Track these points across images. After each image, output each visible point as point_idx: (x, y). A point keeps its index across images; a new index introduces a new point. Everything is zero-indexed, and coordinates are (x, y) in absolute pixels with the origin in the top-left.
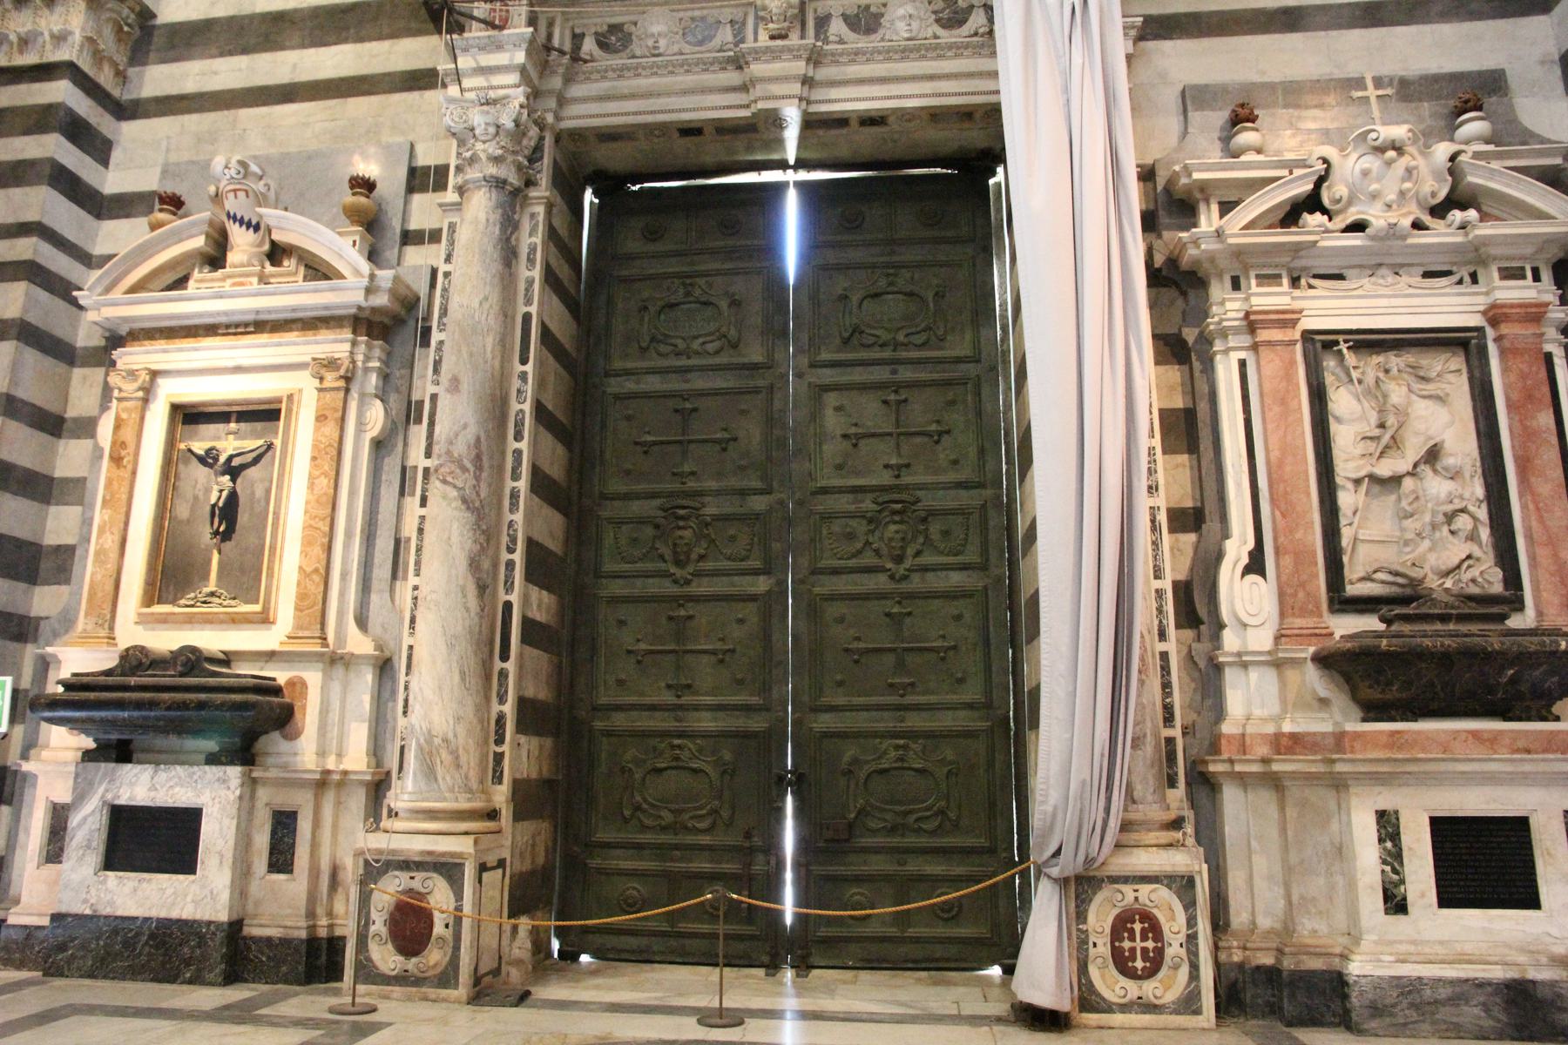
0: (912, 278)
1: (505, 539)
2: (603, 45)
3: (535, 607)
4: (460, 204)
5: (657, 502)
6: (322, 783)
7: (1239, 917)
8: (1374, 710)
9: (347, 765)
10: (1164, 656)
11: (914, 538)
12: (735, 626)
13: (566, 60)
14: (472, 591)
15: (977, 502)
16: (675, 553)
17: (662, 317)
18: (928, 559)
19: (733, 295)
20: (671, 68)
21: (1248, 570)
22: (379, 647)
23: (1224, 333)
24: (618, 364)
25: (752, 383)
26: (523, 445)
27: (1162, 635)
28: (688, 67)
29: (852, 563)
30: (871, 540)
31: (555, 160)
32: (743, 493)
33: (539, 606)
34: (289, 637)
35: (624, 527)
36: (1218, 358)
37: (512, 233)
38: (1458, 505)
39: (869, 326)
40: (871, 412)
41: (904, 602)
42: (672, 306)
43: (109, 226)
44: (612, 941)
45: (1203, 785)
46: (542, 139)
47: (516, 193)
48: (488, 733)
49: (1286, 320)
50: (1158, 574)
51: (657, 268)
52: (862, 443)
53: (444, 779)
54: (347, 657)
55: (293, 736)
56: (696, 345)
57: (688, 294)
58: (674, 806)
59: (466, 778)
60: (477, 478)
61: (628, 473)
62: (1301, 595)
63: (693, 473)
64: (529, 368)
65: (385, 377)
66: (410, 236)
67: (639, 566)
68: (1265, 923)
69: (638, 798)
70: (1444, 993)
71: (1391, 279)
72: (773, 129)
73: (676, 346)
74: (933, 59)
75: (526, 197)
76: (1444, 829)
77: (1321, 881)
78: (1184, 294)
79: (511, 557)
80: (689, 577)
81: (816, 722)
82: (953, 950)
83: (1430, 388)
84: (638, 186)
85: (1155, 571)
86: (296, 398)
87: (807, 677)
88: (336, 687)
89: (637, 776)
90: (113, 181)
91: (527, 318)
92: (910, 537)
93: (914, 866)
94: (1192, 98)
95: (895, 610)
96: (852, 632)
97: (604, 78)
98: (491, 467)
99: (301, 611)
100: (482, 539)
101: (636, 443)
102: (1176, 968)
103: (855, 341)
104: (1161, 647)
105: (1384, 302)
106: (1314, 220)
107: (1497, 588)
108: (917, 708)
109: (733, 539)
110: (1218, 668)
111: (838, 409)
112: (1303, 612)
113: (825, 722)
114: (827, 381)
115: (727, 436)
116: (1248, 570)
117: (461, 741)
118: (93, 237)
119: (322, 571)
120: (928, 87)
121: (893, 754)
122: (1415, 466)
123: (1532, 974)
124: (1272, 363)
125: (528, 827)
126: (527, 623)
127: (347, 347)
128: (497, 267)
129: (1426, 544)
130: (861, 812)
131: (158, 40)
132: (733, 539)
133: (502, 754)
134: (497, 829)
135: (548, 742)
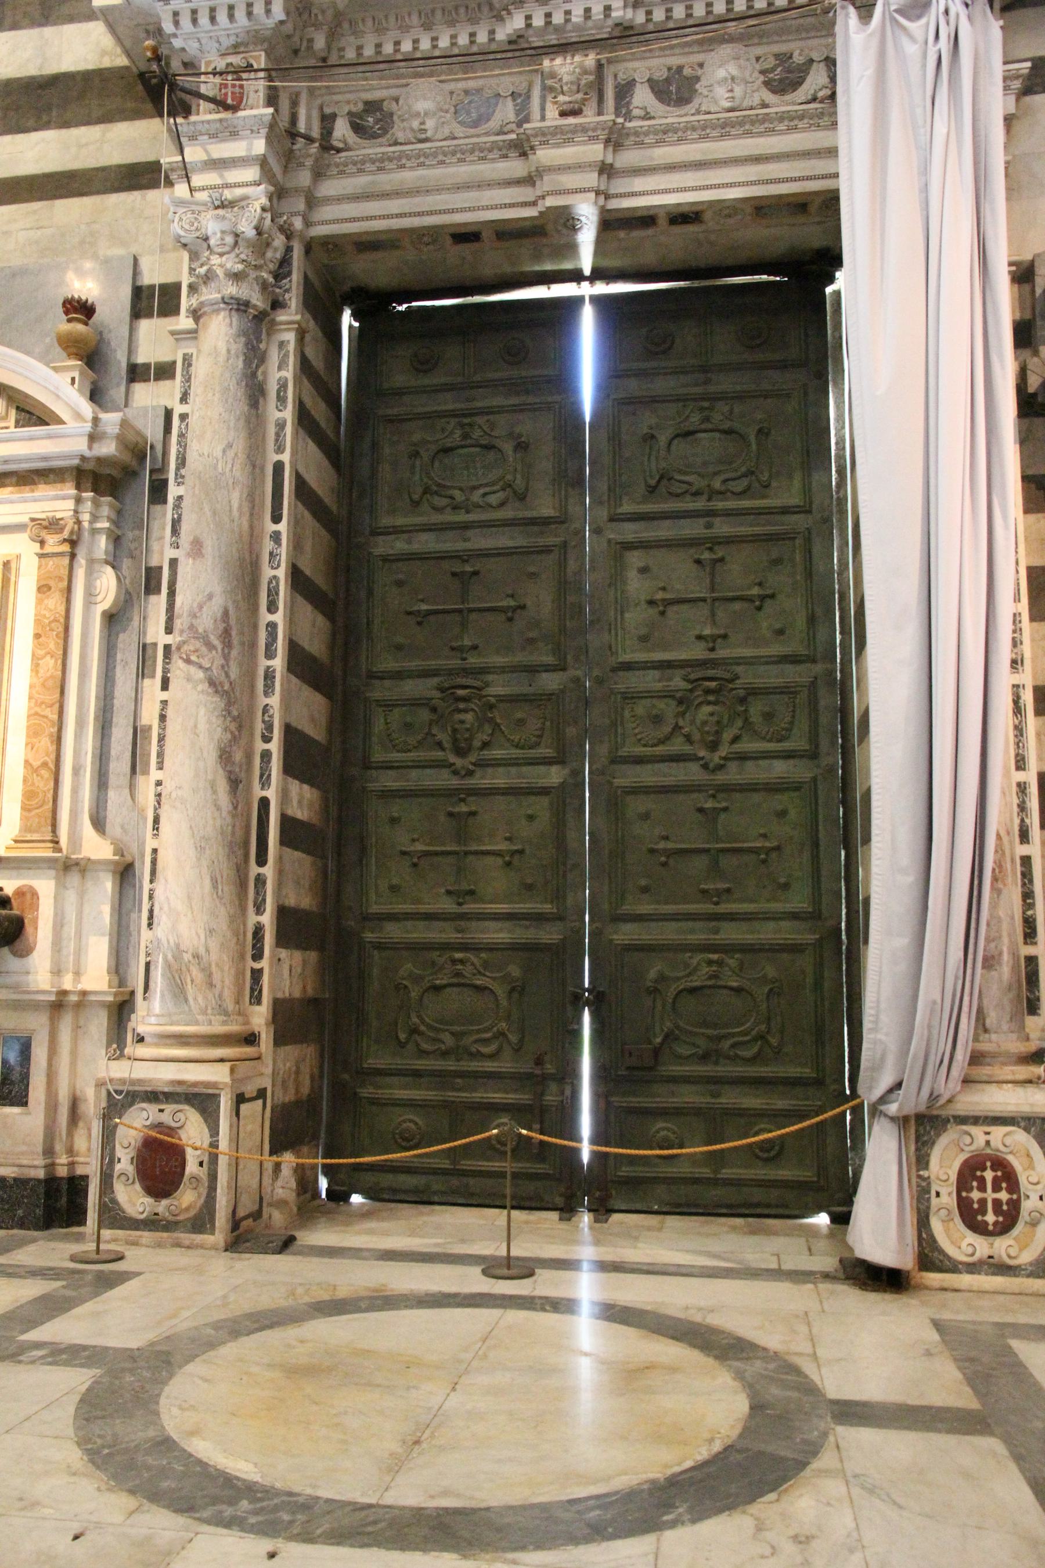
0: (731, 411)
1: (259, 727)
2: (358, 128)
3: (295, 803)
4: (196, 331)
5: (435, 681)
6: (58, 1004)
9: (86, 985)
10: (1026, 861)
11: (731, 720)
12: (524, 822)
13: (314, 148)
14: (223, 786)
15: (806, 680)
16: (455, 741)
17: (437, 464)
19: (520, 436)
20: (441, 157)
22: (119, 851)
24: (386, 521)
25: (542, 541)
26: (278, 617)
27: (1024, 836)
28: (462, 154)
29: (660, 750)
30: (681, 723)
31: (306, 277)
32: (532, 670)
33: (300, 802)
34: (16, 841)
35: (396, 711)
37: (258, 367)
39: (680, 472)
41: (720, 796)
42: (447, 450)
44: (387, 1180)
46: (289, 249)
47: (260, 317)
48: (244, 946)
50: (1021, 764)
52: (672, 611)
53: (195, 999)
54: (83, 863)
55: (25, 953)
56: (476, 497)
57: (465, 436)
58: (457, 1028)
59: (220, 996)
60: (226, 657)
61: (399, 648)
63: (475, 647)
64: (282, 527)
65: (116, 540)
66: (138, 371)
72: (564, 231)
73: (452, 498)
74: (760, 134)
75: (273, 323)
79: (266, 746)
80: (471, 767)
81: (616, 933)
84: (405, 306)
85: (1017, 762)
86: (13, 565)
87: (607, 881)
88: (71, 897)
89: (413, 994)
91: (278, 467)
92: (725, 721)
95: (709, 805)
96: (657, 832)
97: (360, 171)
98: (243, 644)
99: (29, 810)
100: (233, 727)
101: (409, 613)
103: (662, 489)
104: (1022, 850)
108: (731, 917)
109: (521, 722)
111: (644, 570)
113: (625, 934)
114: (630, 537)
115: (512, 603)
117: (214, 957)
119: (52, 766)
120: (752, 172)
121: (705, 969)
125: (291, 1052)
126: (286, 821)
127: (70, 504)
128: (243, 407)
133: (260, 971)
134: (256, 1055)
135: (313, 956)
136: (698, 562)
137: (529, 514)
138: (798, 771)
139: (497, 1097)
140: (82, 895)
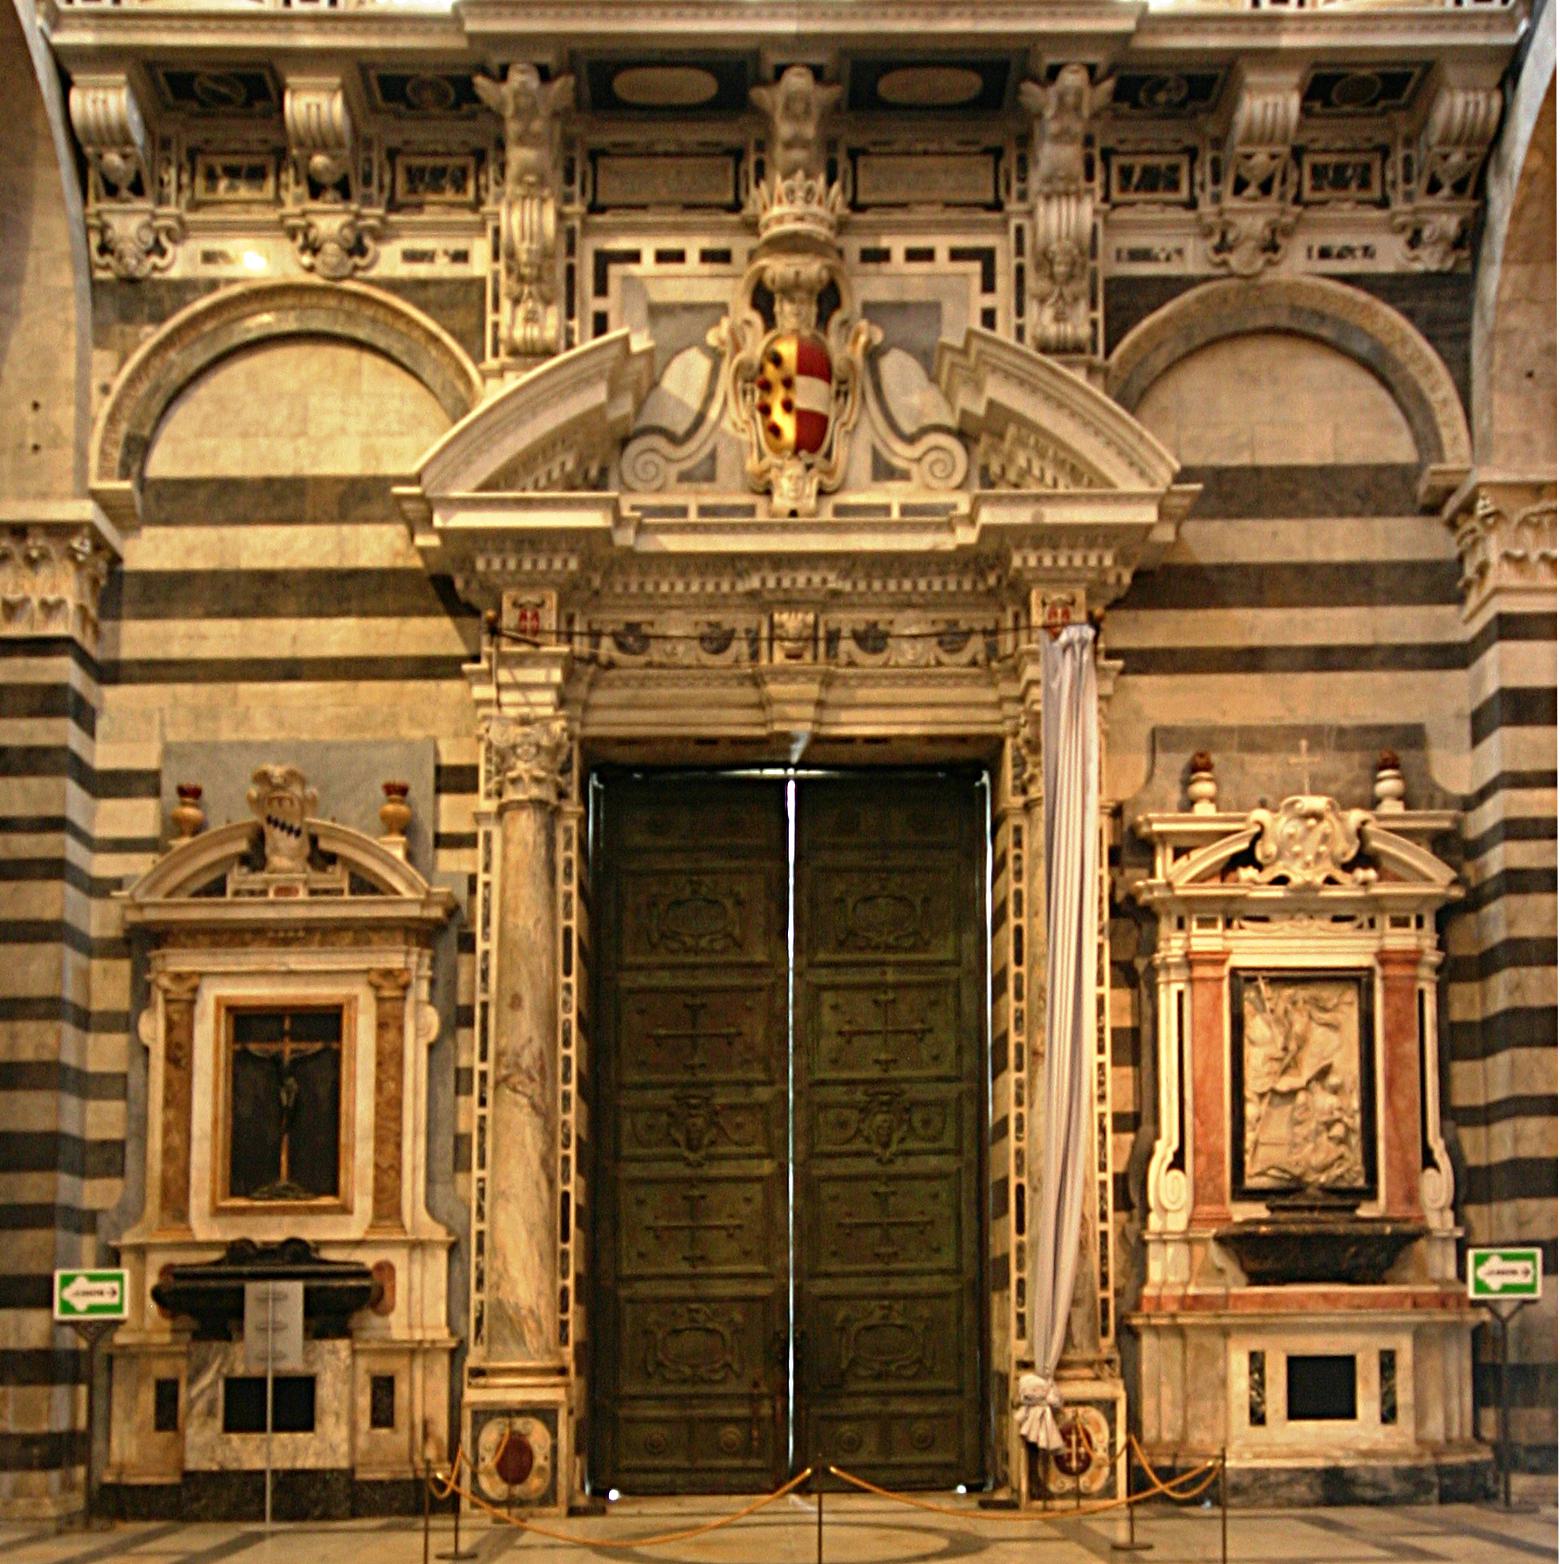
7: (1149, 1434)
8: (1255, 1279)
9: (430, 1335)
10: (1104, 1235)
11: (900, 1124)
14: (544, 1184)
15: (954, 1095)
18: (910, 1145)
21: (1171, 1166)
23: (1167, 967)
27: (1103, 1217)
36: (1162, 987)
38: (1337, 1115)
40: (863, 1009)
43: (108, 805)
44: (642, 1478)
45: (1128, 1334)
49: (1217, 959)
50: (1103, 1167)
51: (665, 865)
60: (543, 1086)
62: (1210, 1188)
68: (1167, 1436)
70: (1283, 1477)
71: (1306, 922)
76: (1296, 1365)
78: (1139, 926)
82: (927, 1474)
83: (1326, 1017)
90: (104, 756)
91: (568, 932)
93: (896, 1405)
94: (1161, 739)
95: (882, 1189)
96: (845, 1209)
102: (1100, 1467)
104: (1101, 1227)
105: (1298, 943)
106: (1247, 873)
107: (1361, 1183)
109: (739, 1126)
110: (1144, 1244)
112: (1211, 1201)
113: (822, 1286)
114: (824, 980)
116: (1171, 1166)
118: (92, 814)
121: (879, 1313)
123: (1346, 1463)
124: (1204, 994)
129: (1310, 1146)
130: (853, 1363)
131: (130, 591)
136: (876, 1002)
137: (745, 959)
138: (948, 1163)
139: (724, 1412)
140: (424, 1265)
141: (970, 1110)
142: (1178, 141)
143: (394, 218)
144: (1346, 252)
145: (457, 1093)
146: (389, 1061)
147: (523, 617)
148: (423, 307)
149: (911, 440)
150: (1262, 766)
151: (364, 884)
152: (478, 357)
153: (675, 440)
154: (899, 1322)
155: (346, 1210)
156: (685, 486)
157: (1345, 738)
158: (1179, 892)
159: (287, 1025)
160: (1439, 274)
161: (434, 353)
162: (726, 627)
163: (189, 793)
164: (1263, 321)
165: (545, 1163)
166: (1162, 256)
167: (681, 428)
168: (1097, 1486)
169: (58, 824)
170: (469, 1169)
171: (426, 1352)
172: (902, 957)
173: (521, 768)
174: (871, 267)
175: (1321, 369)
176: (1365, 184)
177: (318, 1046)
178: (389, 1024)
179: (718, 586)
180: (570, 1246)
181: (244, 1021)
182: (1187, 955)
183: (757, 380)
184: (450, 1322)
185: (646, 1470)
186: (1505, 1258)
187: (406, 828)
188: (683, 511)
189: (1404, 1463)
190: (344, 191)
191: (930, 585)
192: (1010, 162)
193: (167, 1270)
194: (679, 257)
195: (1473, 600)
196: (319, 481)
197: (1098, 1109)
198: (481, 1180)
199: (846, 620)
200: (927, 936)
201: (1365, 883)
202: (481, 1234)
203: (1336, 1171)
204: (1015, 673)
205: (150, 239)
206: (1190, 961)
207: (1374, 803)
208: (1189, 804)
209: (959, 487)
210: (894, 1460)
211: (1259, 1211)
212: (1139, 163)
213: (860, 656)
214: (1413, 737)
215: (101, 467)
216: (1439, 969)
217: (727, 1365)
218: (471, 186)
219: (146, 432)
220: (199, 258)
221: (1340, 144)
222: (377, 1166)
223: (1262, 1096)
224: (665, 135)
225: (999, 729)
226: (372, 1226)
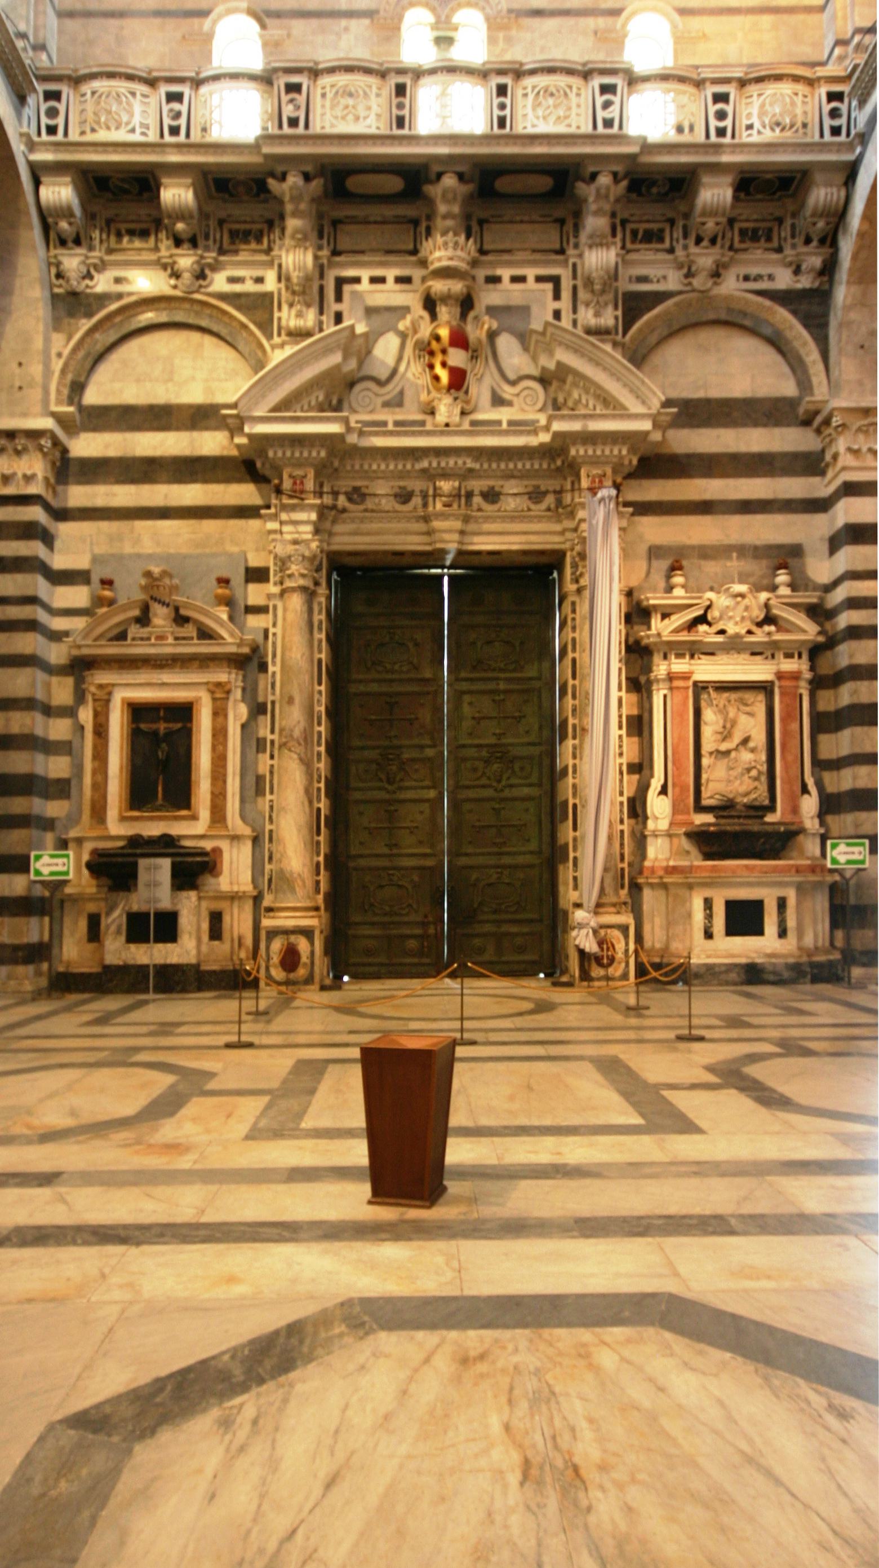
7: (648, 943)
8: (708, 856)
9: (243, 888)
10: (622, 832)
14: (306, 803)
18: (514, 781)
21: (660, 793)
23: (658, 681)
27: (622, 822)
36: (654, 692)
38: (753, 764)
40: (486, 704)
44: (361, 969)
45: (636, 888)
49: (686, 676)
50: (621, 794)
60: (306, 748)
62: (682, 805)
67: (369, 784)
68: (658, 945)
69: (372, 900)
70: (723, 969)
71: (736, 656)
76: (731, 906)
77: (681, 927)
78: (642, 658)
83: (747, 709)
90: (59, 562)
91: (320, 661)
93: (505, 928)
94: (654, 552)
95: (497, 806)
102: (620, 963)
104: (621, 827)
105: (731, 667)
106: (703, 628)
107: (767, 802)
108: (508, 854)
109: (416, 771)
110: (644, 837)
112: (682, 812)
113: (463, 861)
116: (660, 793)
118: (52, 594)
120: (523, 538)
121: (495, 876)
122: (738, 746)
123: (758, 961)
124: (678, 696)
129: (738, 782)
130: (481, 904)
131: (73, 469)
132: (416, 771)
137: (419, 676)
138: (534, 792)
139: (408, 932)
141: (546, 762)
142: (664, 215)
143: (222, 258)
144: (758, 278)
145: (258, 752)
146: (219, 734)
147: (295, 483)
148: (239, 308)
149: (513, 383)
150: (712, 568)
151: (205, 634)
152: (269, 337)
153: (380, 383)
154: (507, 881)
155: (195, 818)
156: (386, 410)
157: (758, 552)
158: (664, 639)
159: (162, 713)
160: (811, 290)
161: (245, 334)
162: (409, 489)
163: (107, 583)
164: (712, 316)
165: (307, 791)
166: (655, 280)
167: (383, 375)
168: (619, 973)
169: (32, 600)
170: (264, 795)
171: (240, 898)
172: (508, 675)
173: (294, 568)
174: (491, 286)
175: (744, 344)
176: (769, 239)
177: (179, 725)
178: (219, 713)
179: (404, 466)
180: (321, 838)
181: (138, 711)
182: (669, 674)
183: (427, 350)
184: (254, 881)
185: (364, 965)
186: (848, 845)
187: (229, 602)
188: (385, 424)
189: (791, 960)
190: (194, 242)
191: (524, 466)
192: (569, 226)
193: (95, 852)
194: (382, 280)
195: (830, 474)
196: (180, 408)
197: (618, 761)
198: (271, 801)
199: (477, 485)
200: (522, 663)
201: (769, 634)
202: (271, 831)
203: (753, 796)
204: (572, 515)
205: (84, 270)
206: (671, 677)
207: (773, 588)
208: (670, 589)
209: (541, 410)
210: (504, 959)
211: (709, 818)
212: (642, 227)
213: (485, 506)
214: (796, 551)
215: (57, 399)
216: (811, 682)
217: (410, 906)
218: (265, 241)
219: (82, 379)
220: (112, 280)
221: (755, 217)
222: (212, 793)
223: (711, 753)
224: (377, 211)
225: (562, 547)
226: (209, 827)
